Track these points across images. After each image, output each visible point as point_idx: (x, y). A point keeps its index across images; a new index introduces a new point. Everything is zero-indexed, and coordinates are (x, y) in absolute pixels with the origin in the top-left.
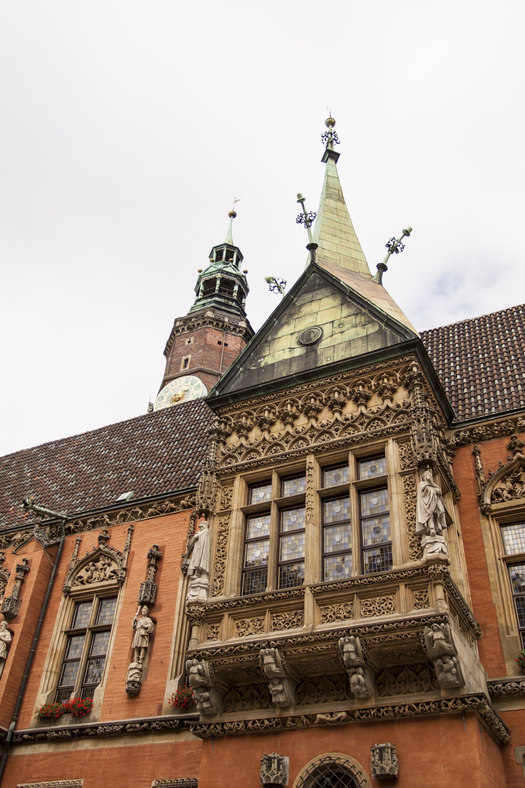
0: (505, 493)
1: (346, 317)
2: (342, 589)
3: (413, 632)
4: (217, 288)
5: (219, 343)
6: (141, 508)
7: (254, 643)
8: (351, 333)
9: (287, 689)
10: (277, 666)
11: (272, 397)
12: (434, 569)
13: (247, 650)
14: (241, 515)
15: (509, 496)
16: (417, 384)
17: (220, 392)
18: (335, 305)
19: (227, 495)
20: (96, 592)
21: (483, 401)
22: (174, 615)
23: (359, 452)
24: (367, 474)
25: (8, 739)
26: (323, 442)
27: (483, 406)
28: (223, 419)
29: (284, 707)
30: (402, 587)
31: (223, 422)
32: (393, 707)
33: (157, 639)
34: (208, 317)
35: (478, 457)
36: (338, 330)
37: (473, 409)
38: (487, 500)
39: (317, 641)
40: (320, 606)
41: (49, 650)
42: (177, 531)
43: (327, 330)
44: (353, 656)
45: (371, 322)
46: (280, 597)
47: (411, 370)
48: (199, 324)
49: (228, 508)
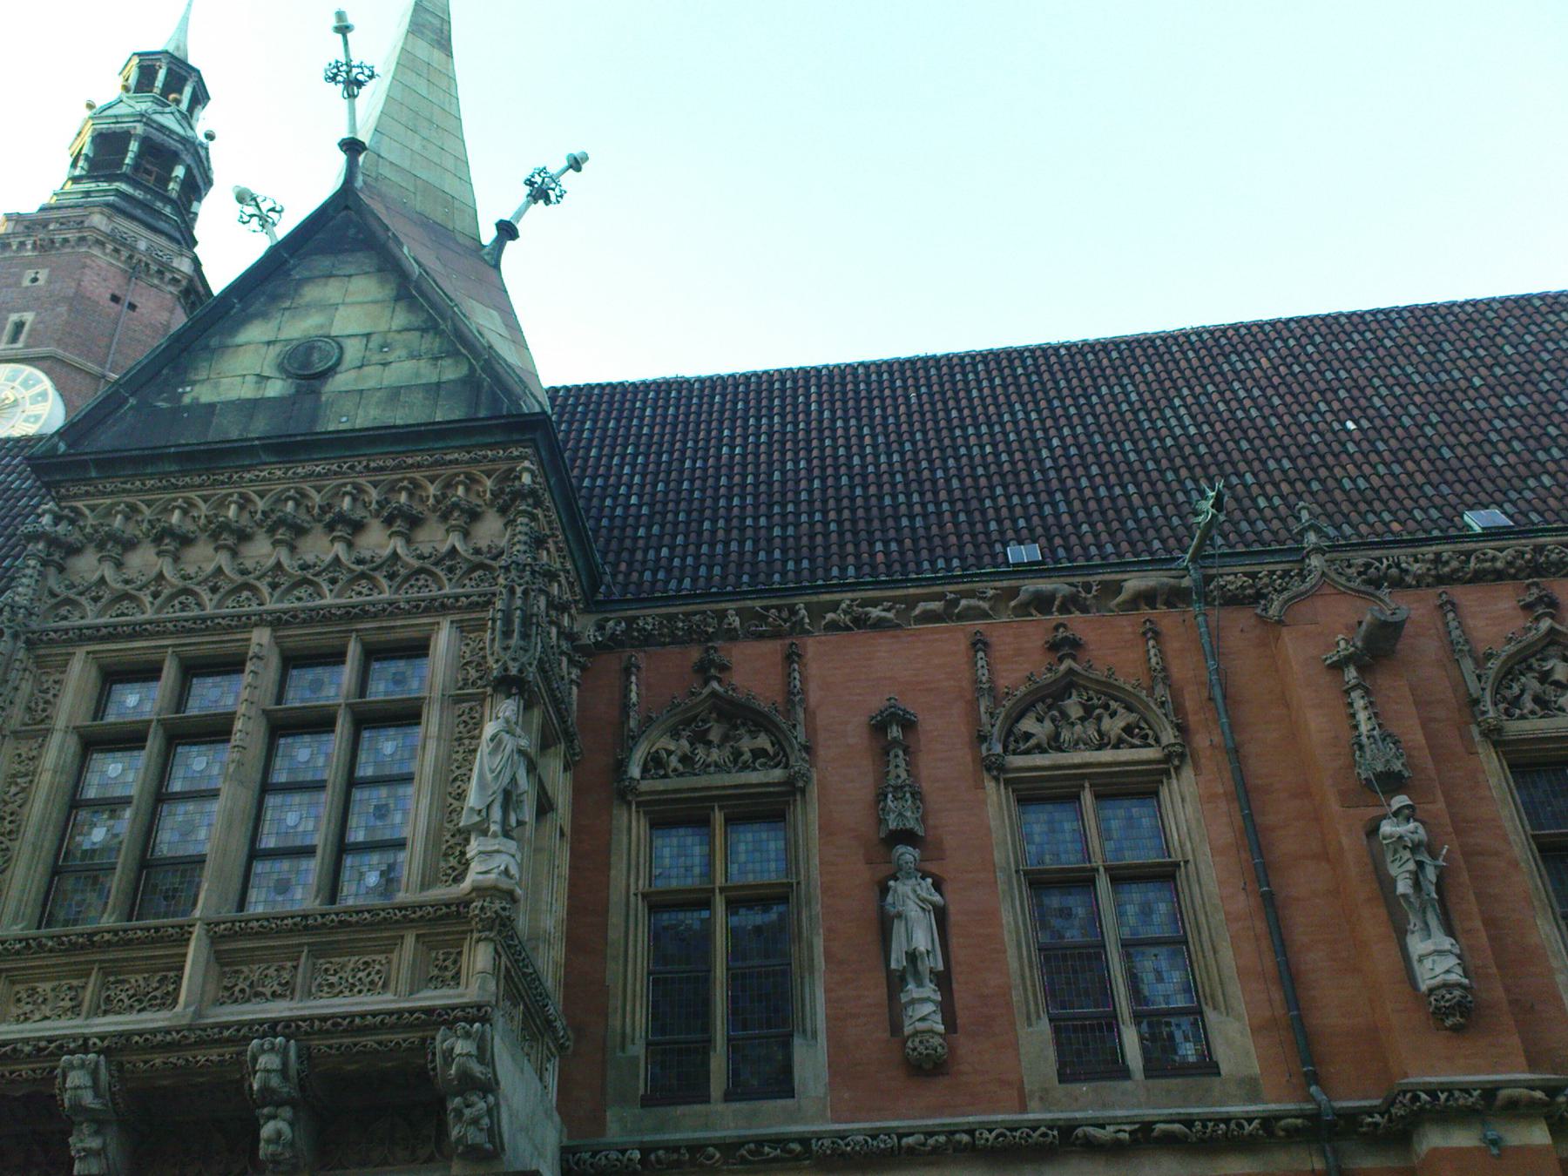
0: (674, 761)
1: (399, 332)
2: (279, 932)
3: (415, 1037)
4: (127, 161)
5: (115, 299)
7: (50, 1040)
8: (402, 371)
9: (112, 1150)
10: (97, 1095)
11: (197, 480)
12: (482, 908)
13: (29, 1055)
14: (73, 744)
15: (680, 767)
16: (525, 511)
17: (69, 446)
18: (380, 297)
19: (46, 691)
21: (671, 560)
24: (382, 687)
26: (297, 604)
27: (669, 570)
28: (66, 512)
30: (410, 940)
31: (67, 517)
34: (93, 228)
35: (633, 678)
36: (376, 358)
37: (647, 575)
38: (635, 771)
39: (200, 1043)
40: (222, 965)
43: (353, 350)
44: (275, 1081)
46: (131, 940)
47: (519, 478)
48: (66, 240)
49: (42, 721)
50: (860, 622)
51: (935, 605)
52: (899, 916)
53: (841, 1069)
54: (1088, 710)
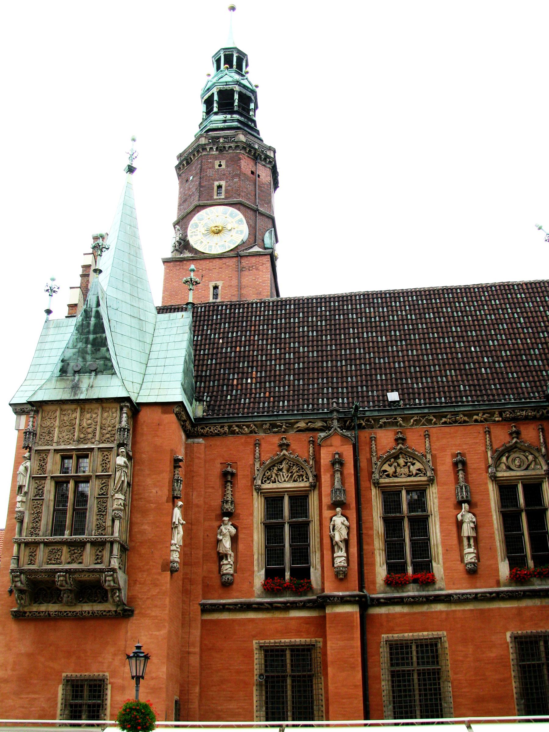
6: (434, 416)
22: (491, 512)
33: (480, 530)
41: (375, 532)
48: (230, 147)
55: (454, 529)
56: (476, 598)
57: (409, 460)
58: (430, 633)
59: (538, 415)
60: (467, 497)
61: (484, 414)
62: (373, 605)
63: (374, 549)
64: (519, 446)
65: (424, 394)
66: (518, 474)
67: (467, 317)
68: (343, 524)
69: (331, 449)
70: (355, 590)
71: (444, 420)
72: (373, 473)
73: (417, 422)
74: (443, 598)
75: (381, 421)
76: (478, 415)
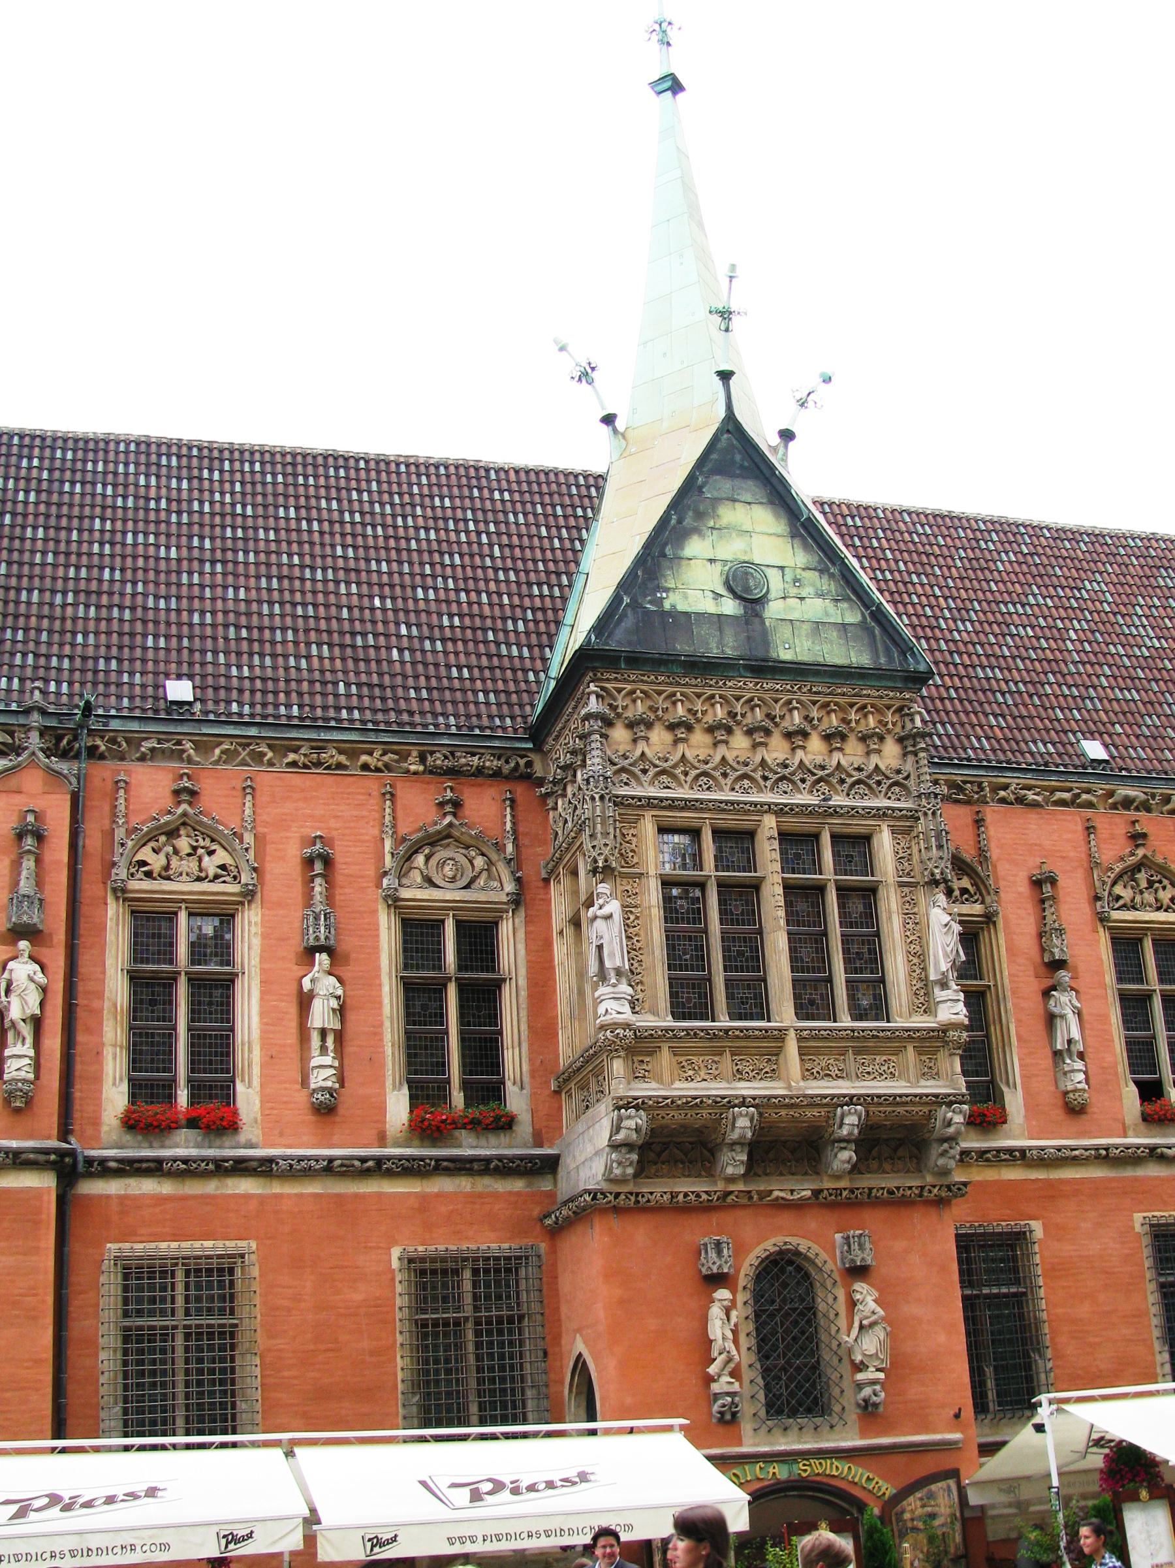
6: (270, 746)
7: (723, 1097)
11: (693, 682)
20: (183, 901)
22: (379, 976)
23: (837, 829)
25: (81, 1167)
29: (731, 1179)
30: (910, 1049)
32: (870, 1189)
33: (351, 1016)
36: (793, 591)
41: (107, 1005)
42: (356, 813)
43: (775, 582)
45: (849, 599)
50: (1020, 800)
51: (1066, 796)
52: (1063, 1017)
53: (1031, 1107)
54: (1151, 884)
55: (293, 1010)
56: (330, 1169)
57: (202, 843)
58: (220, 1244)
59: (506, 769)
60: (327, 938)
61: (384, 753)
62: (90, 1175)
63: (103, 1044)
64: (456, 834)
65: (253, 692)
66: (449, 896)
67: (374, 527)
68: (31, 979)
69: (17, 799)
70: (49, 1138)
71: (292, 757)
72: (114, 864)
73: (229, 755)
74: (255, 1164)
75: (146, 746)
76: (371, 754)
